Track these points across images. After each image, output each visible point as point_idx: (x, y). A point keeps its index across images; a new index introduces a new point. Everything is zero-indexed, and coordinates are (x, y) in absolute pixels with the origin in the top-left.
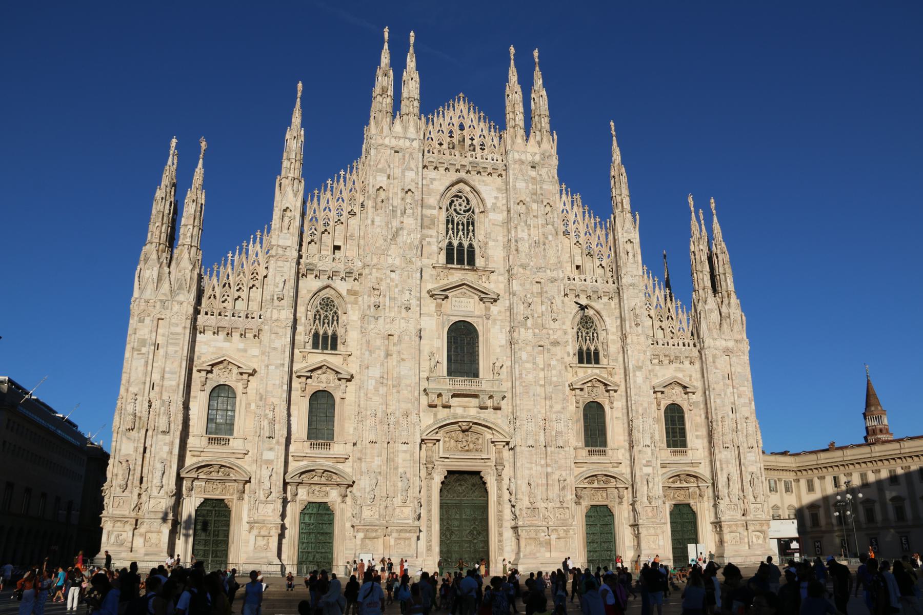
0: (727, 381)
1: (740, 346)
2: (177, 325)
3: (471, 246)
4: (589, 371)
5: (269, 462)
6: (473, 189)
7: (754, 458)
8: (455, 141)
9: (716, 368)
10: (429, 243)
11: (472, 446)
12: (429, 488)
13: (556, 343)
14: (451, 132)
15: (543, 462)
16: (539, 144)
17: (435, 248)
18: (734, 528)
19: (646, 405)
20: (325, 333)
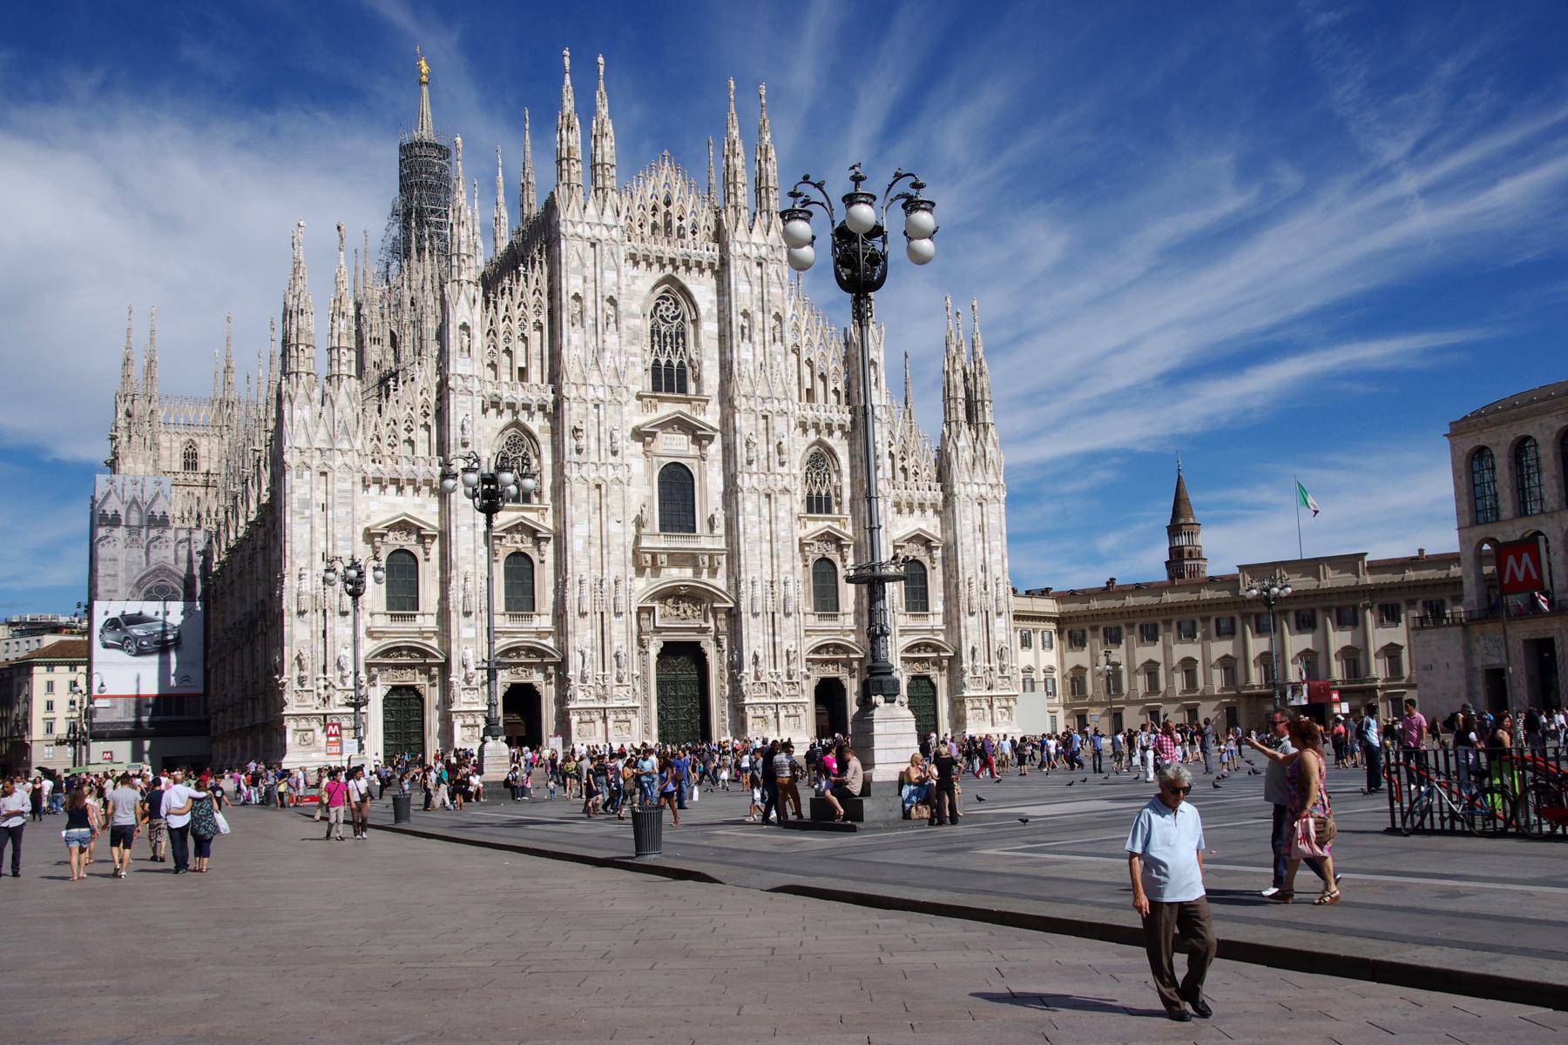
0: (979, 535)
1: (996, 491)
2: (345, 480)
5: (468, 640)
10: (633, 364)
11: (689, 612)
12: (644, 664)
13: (786, 491)
17: (640, 370)
18: (977, 704)
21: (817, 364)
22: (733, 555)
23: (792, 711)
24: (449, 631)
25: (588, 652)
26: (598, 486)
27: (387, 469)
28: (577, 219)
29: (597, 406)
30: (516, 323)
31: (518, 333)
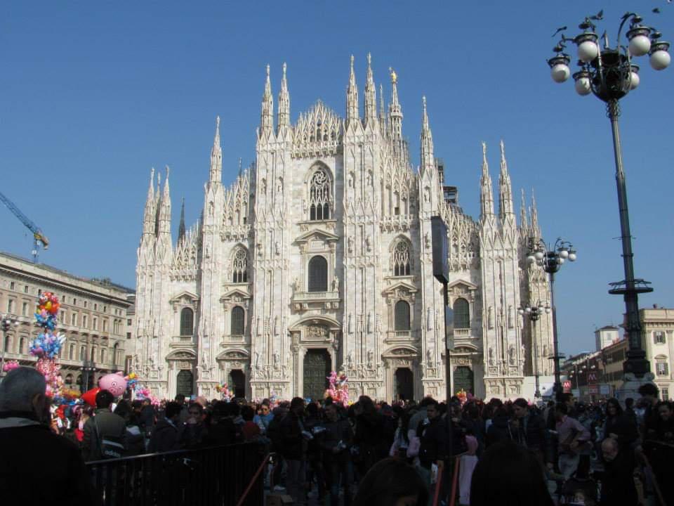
0: (498, 280)
3: (326, 205)
4: (400, 281)
5: (206, 349)
6: (327, 167)
7: (515, 335)
8: (313, 135)
9: (489, 271)
10: (297, 208)
13: (371, 265)
14: (313, 128)
15: (360, 342)
16: (365, 127)
17: (301, 211)
18: (493, 383)
19: (432, 301)
20: (240, 272)
21: (401, 194)
22: (341, 301)
23: (371, 386)
24: (198, 346)
25: (261, 354)
26: (270, 271)
27: (181, 273)
28: (265, 142)
29: (271, 232)
30: (242, 197)
31: (242, 201)
